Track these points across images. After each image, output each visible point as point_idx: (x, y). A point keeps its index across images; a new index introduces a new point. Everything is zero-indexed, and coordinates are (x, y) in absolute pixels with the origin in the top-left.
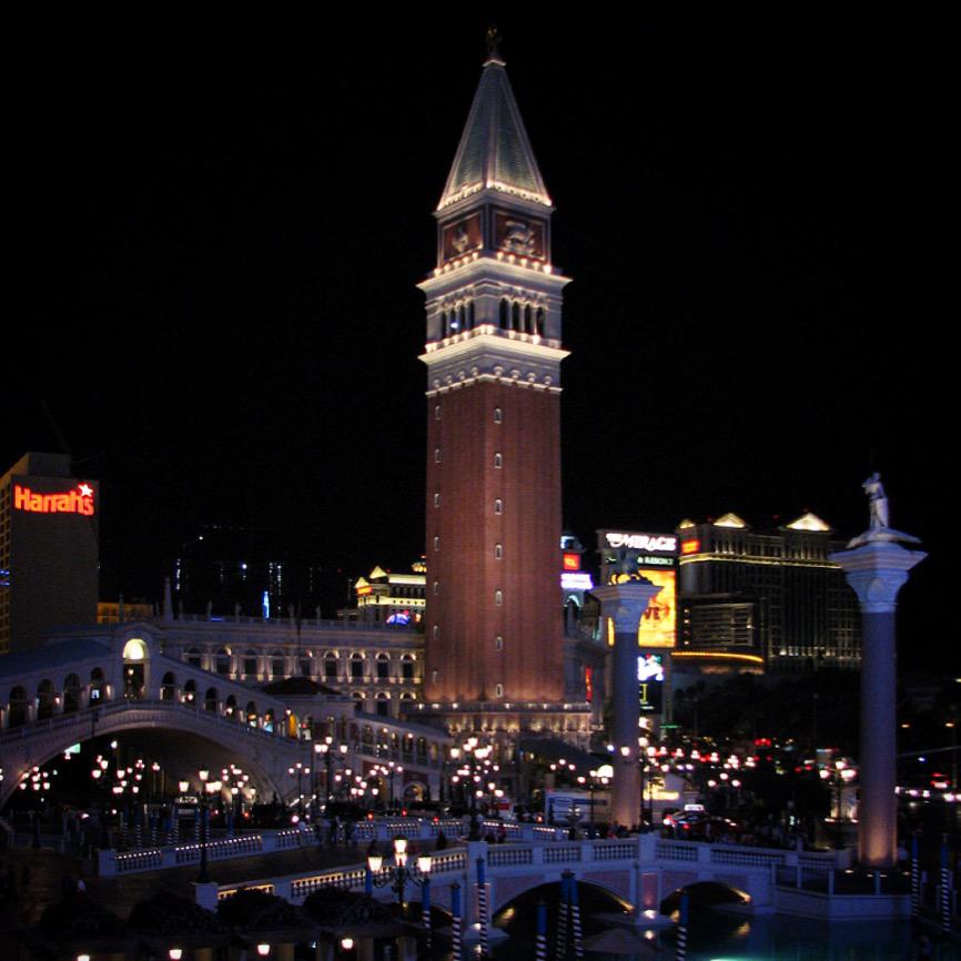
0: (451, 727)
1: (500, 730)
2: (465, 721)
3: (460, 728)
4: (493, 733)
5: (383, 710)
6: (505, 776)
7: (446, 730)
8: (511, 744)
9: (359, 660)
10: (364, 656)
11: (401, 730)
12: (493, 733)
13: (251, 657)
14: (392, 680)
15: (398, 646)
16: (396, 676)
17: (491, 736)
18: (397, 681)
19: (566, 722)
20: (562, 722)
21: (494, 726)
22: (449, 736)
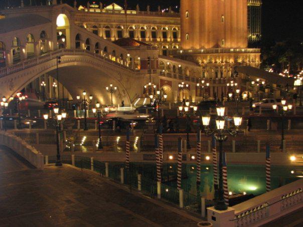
0: (200, 61)
1: (226, 62)
2: (208, 58)
3: (205, 62)
4: (224, 64)
5: (165, 54)
6: (212, 82)
7: (197, 64)
8: (231, 69)
9: (144, 30)
10: (145, 28)
11: (174, 63)
12: (224, 64)
13: (96, 29)
14: (158, 40)
15: (160, 23)
16: (160, 38)
17: (223, 66)
18: (161, 40)
19: (251, 58)
20: (249, 58)
21: (224, 61)
22: (199, 66)
